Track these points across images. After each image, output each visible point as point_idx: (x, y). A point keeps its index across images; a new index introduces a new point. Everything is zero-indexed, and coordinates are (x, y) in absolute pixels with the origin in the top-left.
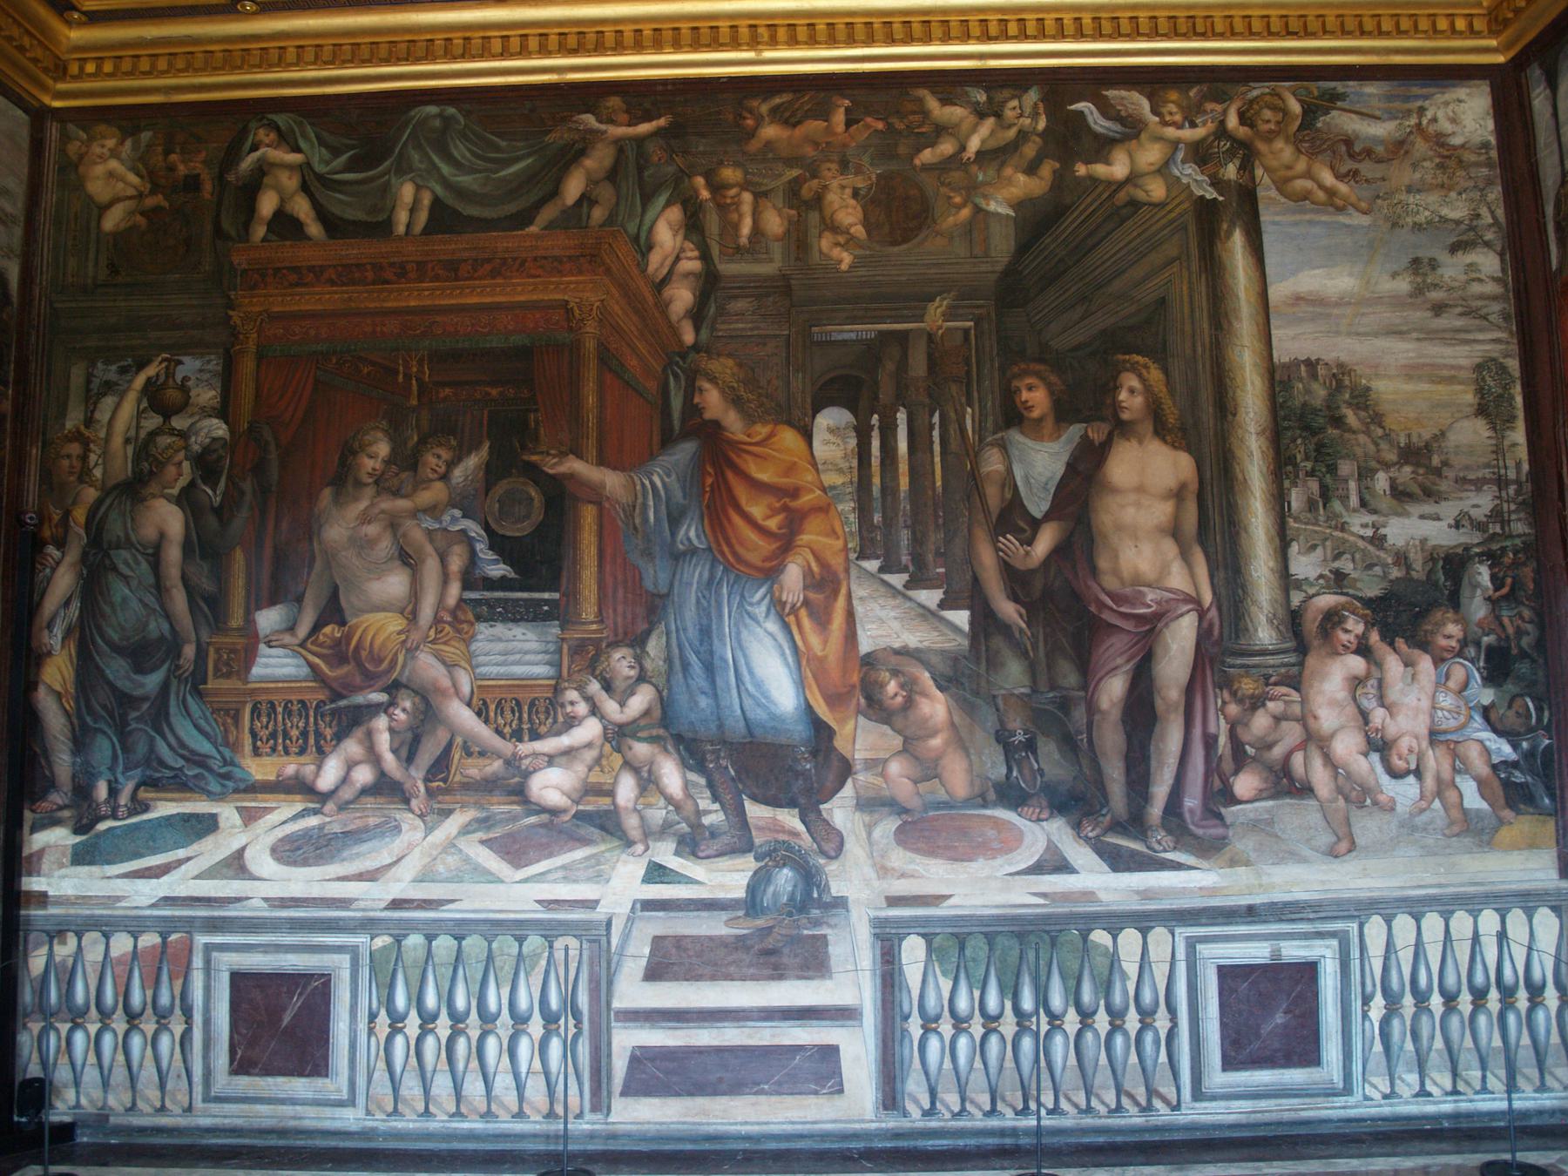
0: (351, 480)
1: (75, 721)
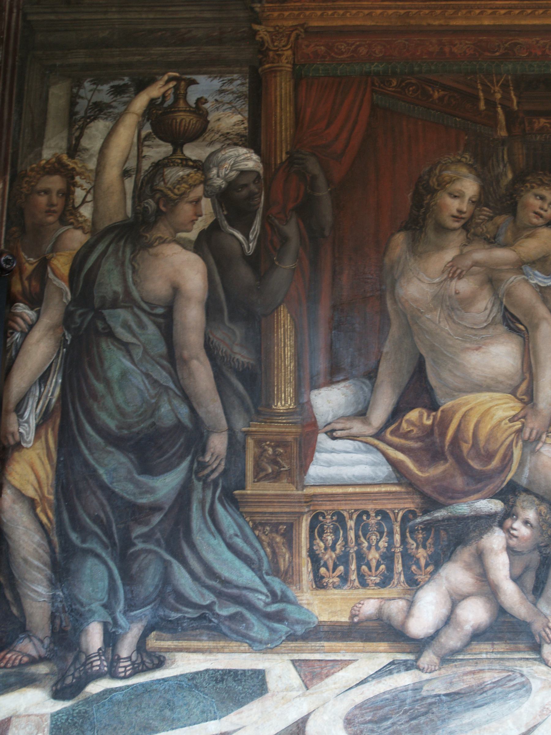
0: (430, 222)
1: (55, 539)
